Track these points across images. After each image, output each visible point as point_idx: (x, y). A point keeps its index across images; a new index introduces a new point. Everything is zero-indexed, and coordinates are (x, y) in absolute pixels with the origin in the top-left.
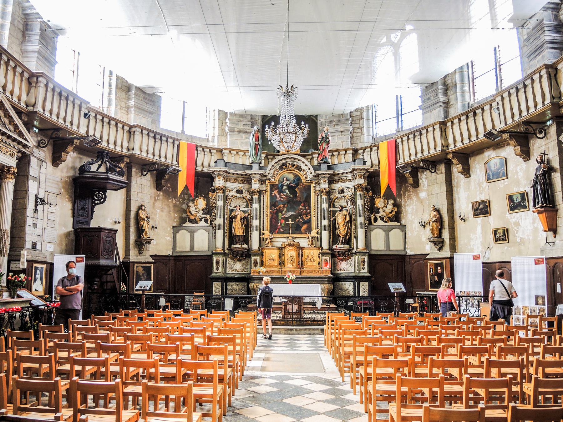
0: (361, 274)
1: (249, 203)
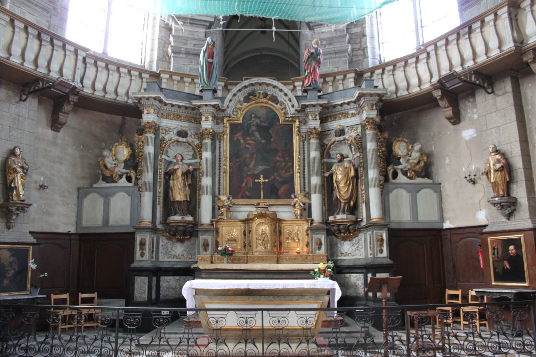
0: (378, 262)
1: (198, 150)
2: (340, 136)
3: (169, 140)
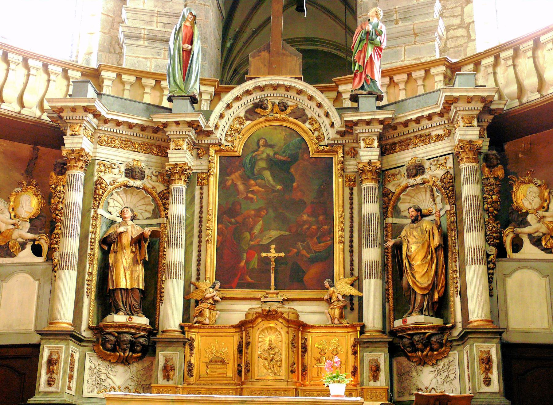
2: (415, 175)
3: (110, 184)
